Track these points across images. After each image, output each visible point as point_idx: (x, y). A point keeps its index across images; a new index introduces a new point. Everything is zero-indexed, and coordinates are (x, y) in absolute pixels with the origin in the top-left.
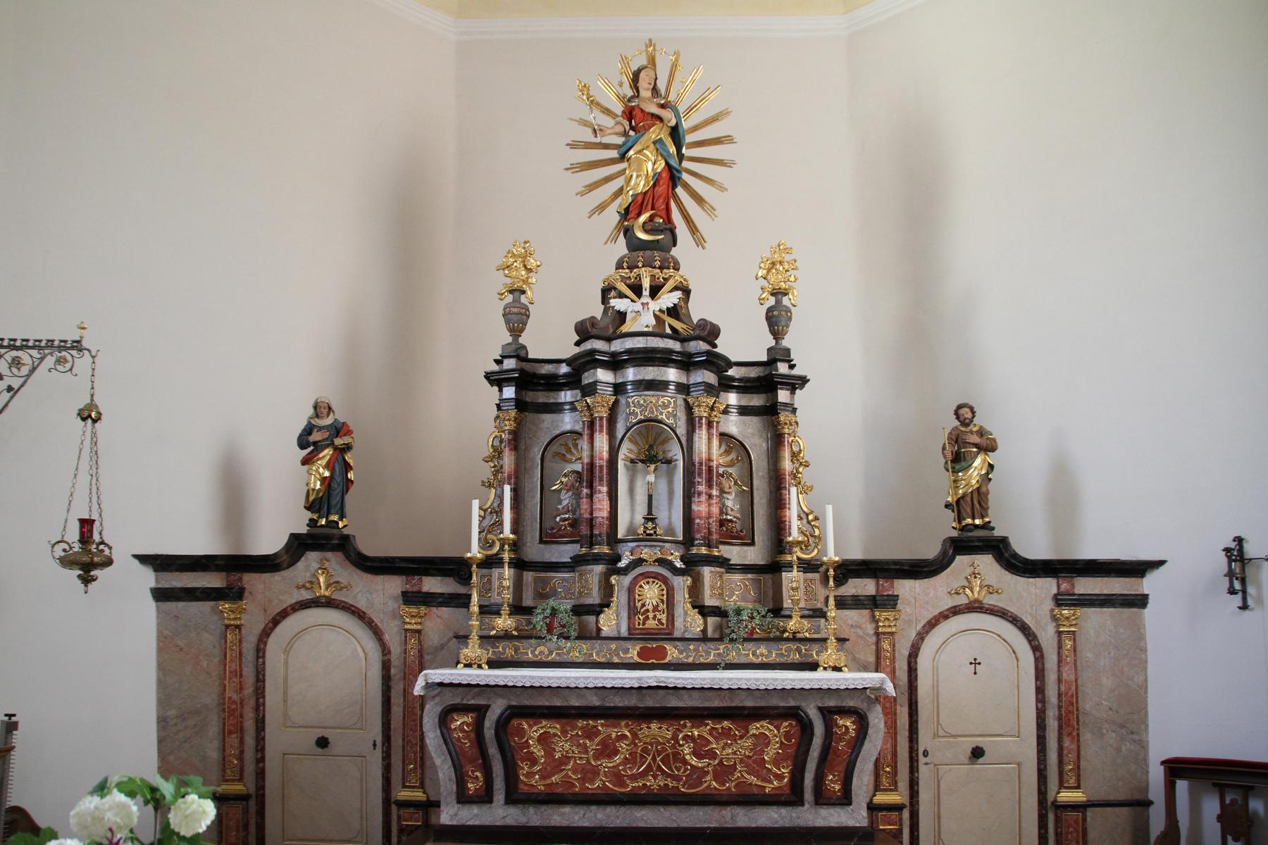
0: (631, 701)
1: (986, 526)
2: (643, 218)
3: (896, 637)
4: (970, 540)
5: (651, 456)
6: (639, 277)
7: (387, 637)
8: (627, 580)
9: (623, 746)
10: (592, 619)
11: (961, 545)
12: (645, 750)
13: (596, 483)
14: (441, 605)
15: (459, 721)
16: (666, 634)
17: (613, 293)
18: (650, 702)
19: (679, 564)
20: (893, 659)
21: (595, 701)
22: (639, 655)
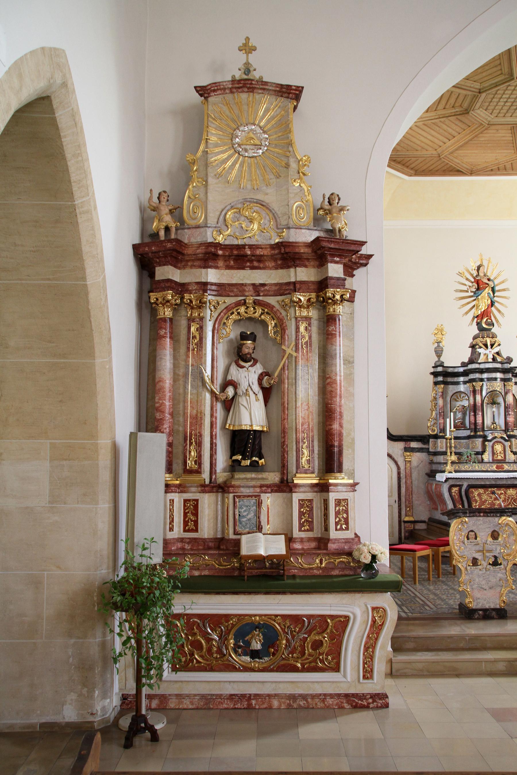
0: (504, 482)
2: (485, 320)
5: (494, 403)
6: (486, 341)
7: (399, 463)
8: (491, 443)
9: (502, 496)
10: (480, 456)
12: (509, 498)
13: (477, 412)
14: (417, 452)
15: (455, 490)
16: (503, 461)
17: (477, 347)
18: (509, 482)
19: (507, 438)
21: (494, 483)
22: (496, 468)
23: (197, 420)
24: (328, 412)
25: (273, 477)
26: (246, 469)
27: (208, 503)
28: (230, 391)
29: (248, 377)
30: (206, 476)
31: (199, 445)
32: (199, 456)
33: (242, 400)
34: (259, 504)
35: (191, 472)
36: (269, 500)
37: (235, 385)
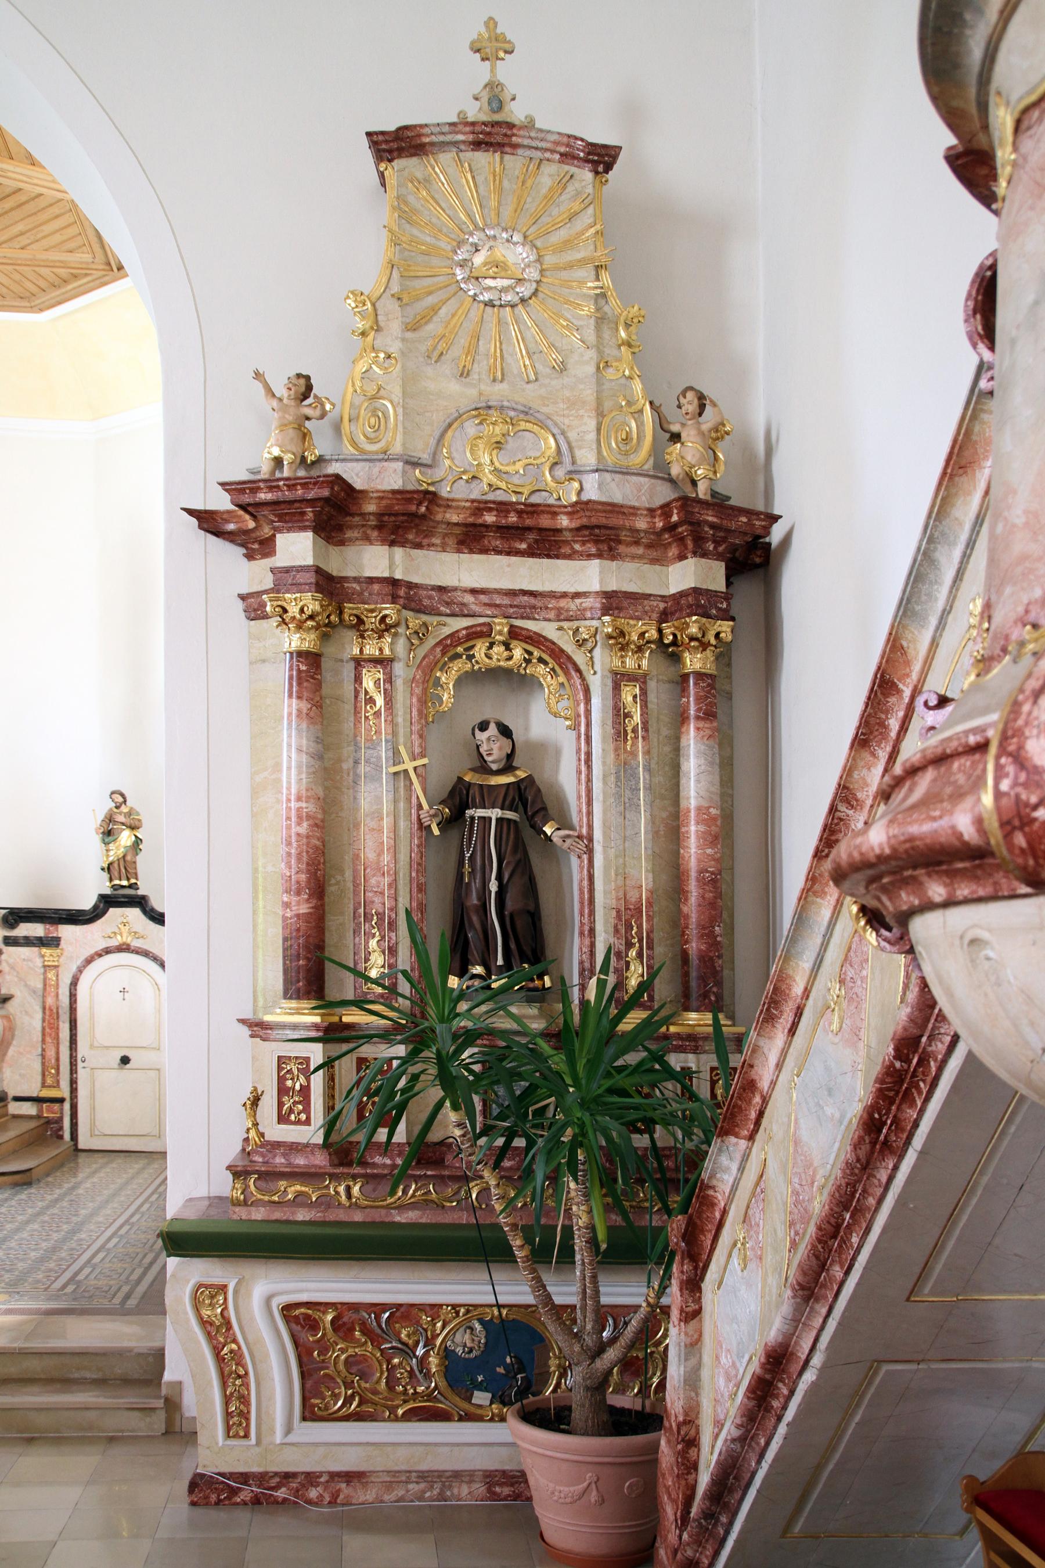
1: (130, 886)
3: (60, 969)
4: (116, 896)
11: (107, 902)
20: (57, 986)
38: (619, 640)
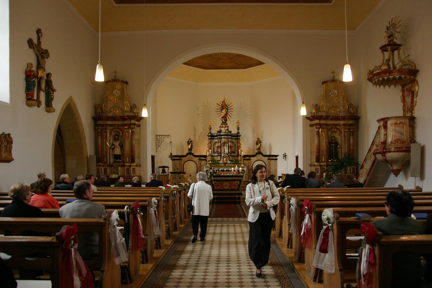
23: (106, 152)
24: (132, 151)
25: (122, 164)
26: (117, 162)
27: (109, 169)
28: (113, 147)
29: (117, 144)
30: (108, 163)
31: (107, 157)
32: (107, 160)
33: (115, 149)
34: (118, 169)
35: (105, 163)
36: (120, 168)
37: (114, 145)
38: (345, 129)
